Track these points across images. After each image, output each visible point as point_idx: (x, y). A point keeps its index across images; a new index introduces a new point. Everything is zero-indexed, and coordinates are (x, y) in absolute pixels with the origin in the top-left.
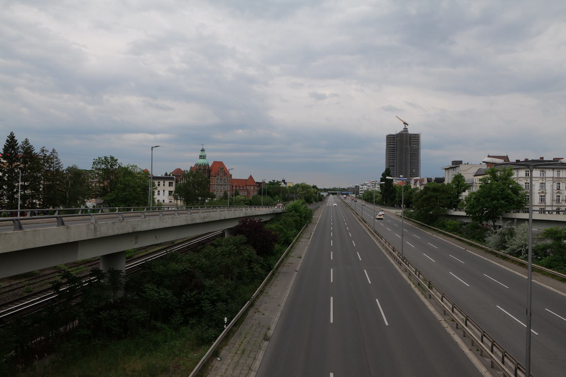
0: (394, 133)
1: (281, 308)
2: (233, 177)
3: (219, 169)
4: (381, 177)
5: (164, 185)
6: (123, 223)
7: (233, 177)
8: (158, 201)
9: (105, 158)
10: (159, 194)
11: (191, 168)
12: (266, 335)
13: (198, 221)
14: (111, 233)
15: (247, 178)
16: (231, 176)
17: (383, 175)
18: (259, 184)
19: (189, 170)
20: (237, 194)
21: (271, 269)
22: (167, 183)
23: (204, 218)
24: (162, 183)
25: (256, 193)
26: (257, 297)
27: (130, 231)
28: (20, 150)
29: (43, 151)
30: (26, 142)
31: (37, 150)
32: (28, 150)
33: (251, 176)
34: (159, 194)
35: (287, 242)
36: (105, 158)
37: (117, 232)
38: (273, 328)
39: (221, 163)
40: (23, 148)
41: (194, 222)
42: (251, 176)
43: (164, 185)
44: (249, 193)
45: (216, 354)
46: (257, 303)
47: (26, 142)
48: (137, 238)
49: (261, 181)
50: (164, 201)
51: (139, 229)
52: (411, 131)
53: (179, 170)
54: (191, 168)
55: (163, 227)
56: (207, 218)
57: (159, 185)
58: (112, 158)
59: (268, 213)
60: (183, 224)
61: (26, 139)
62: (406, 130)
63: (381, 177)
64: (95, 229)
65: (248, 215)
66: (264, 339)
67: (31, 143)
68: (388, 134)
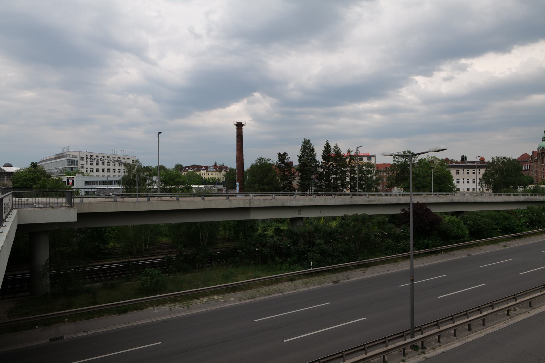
1: (388, 272)
5: (479, 173)
6: (273, 200)
8: (474, 189)
9: (404, 152)
11: (533, 152)
12: (338, 281)
13: (359, 203)
14: (262, 205)
21: (427, 248)
22: (483, 171)
23: (370, 201)
26: (383, 262)
27: (280, 205)
28: (332, 152)
29: (349, 152)
30: (336, 147)
31: (344, 152)
32: (338, 152)
35: (505, 231)
36: (404, 152)
37: (267, 205)
38: (353, 279)
40: (335, 151)
41: (355, 203)
45: (292, 279)
46: (376, 267)
47: (336, 147)
48: (299, 211)
51: (288, 204)
54: (533, 152)
55: (314, 204)
56: (374, 201)
58: (409, 152)
59: (513, 200)
60: (338, 204)
61: (336, 145)
64: (250, 202)
65: (457, 201)
66: (333, 282)
67: (340, 146)
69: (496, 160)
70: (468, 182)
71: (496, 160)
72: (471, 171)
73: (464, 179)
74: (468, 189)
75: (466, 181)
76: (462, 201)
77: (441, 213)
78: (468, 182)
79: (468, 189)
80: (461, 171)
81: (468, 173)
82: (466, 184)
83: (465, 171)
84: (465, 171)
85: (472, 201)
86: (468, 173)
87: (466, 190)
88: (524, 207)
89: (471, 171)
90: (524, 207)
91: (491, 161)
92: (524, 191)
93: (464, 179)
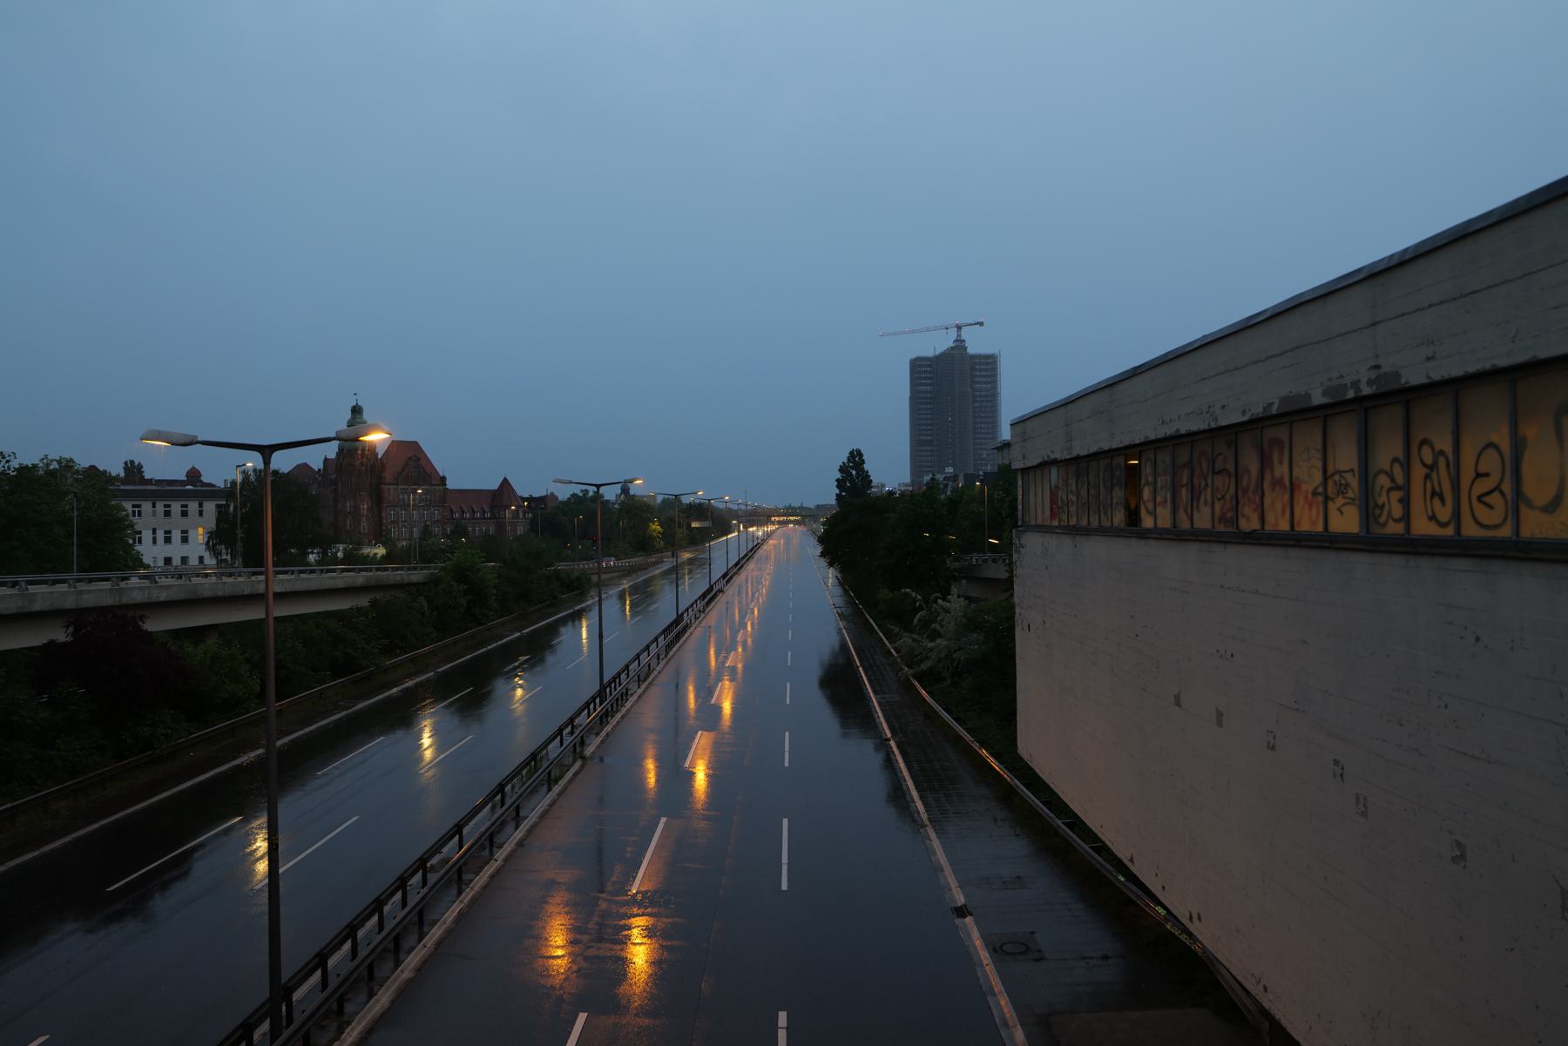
0: (929, 353)
2: (450, 485)
3: (410, 461)
4: (839, 475)
5: (201, 513)
7: (450, 485)
8: (184, 560)
10: (185, 540)
11: (326, 460)
15: (494, 485)
16: (443, 479)
17: (841, 470)
18: (536, 503)
19: (321, 466)
20: (459, 531)
22: (210, 507)
24: (193, 506)
25: (520, 530)
33: (505, 482)
34: (185, 540)
39: (414, 447)
42: (505, 482)
43: (201, 513)
44: (501, 527)
49: (543, 494)
50: (201, 559)
52: (973, 348)
53: (305, 465)
54: (326, 460)
57: (184, 514)
62: (960, 342)
63: (839, 475)
65: (206, 594)
68: (914, 356)
69: (252, 478)
70: (168, 540)
71: (252, 478)
72: (176, 507)
73: (154, 531)
74: (168, 561)
75: (160, 535)
76: (220, 593)
77: (177, 634)
78: (168, 540)
79: (168, 561)
80: (146, 506)
81: (167, 514)
82: (175, 546)
83: (160, 506)
84: (160, 506)
85: (247, 591)
86: (167, 514)
87: (161, 563)
88: (363, 601)
89: (176, 507)
90: (363, 601)
91: (239, 479)
92: (319, 563)
93: (154, 531)
